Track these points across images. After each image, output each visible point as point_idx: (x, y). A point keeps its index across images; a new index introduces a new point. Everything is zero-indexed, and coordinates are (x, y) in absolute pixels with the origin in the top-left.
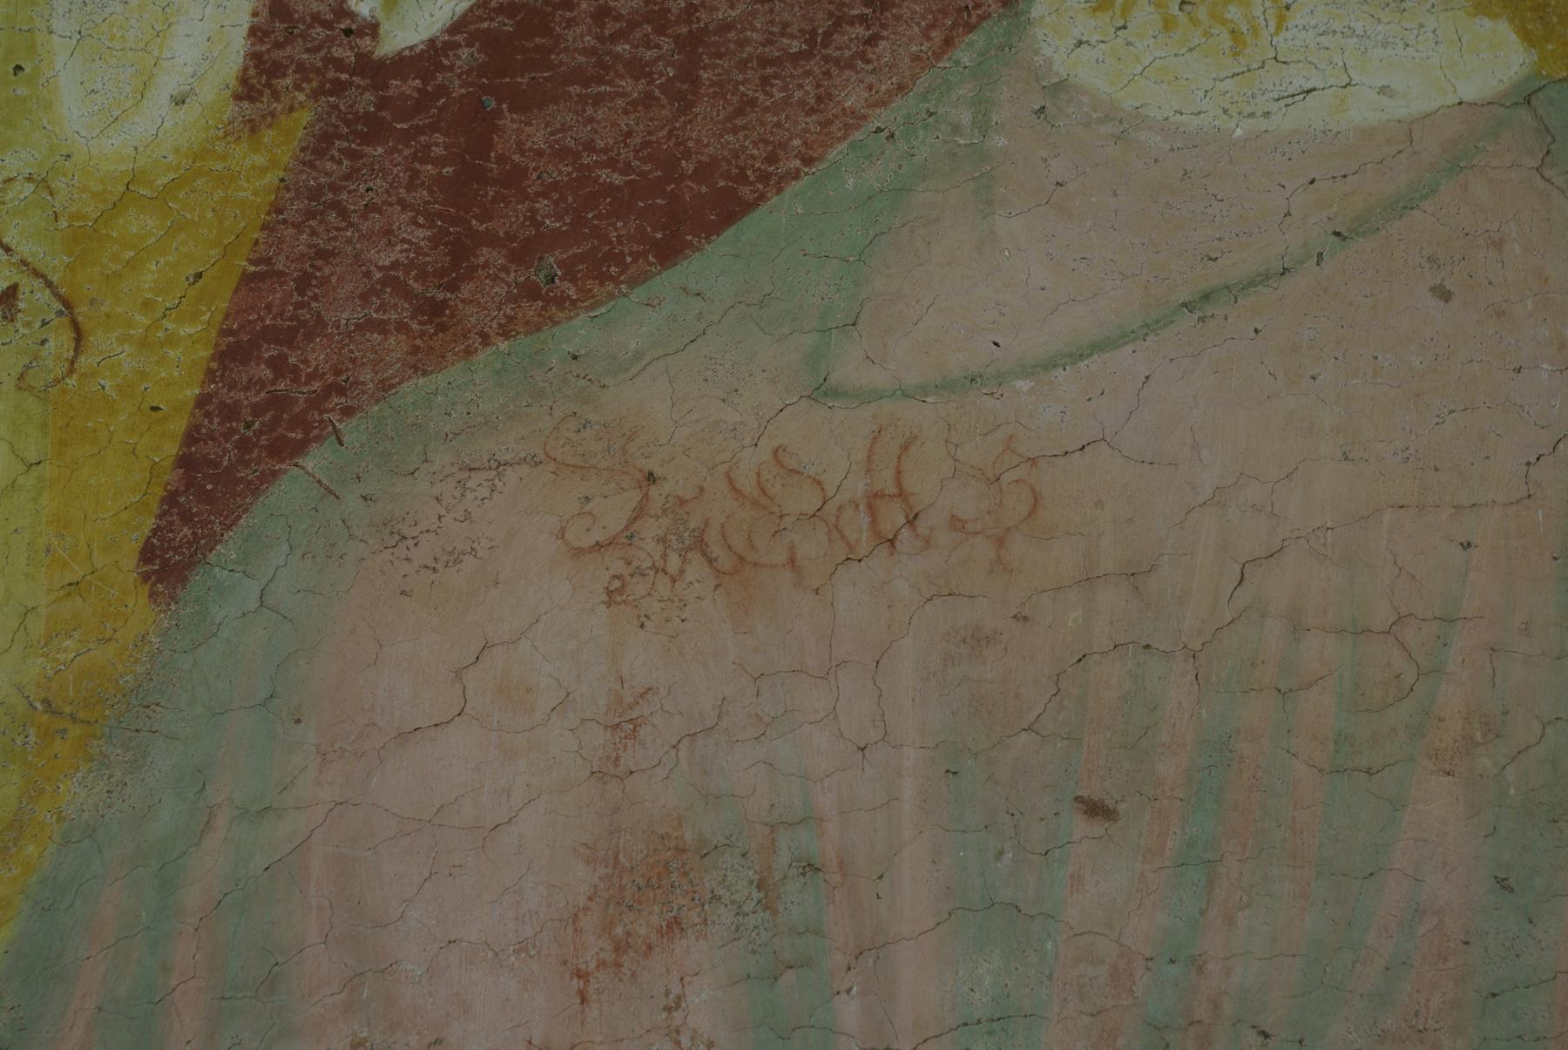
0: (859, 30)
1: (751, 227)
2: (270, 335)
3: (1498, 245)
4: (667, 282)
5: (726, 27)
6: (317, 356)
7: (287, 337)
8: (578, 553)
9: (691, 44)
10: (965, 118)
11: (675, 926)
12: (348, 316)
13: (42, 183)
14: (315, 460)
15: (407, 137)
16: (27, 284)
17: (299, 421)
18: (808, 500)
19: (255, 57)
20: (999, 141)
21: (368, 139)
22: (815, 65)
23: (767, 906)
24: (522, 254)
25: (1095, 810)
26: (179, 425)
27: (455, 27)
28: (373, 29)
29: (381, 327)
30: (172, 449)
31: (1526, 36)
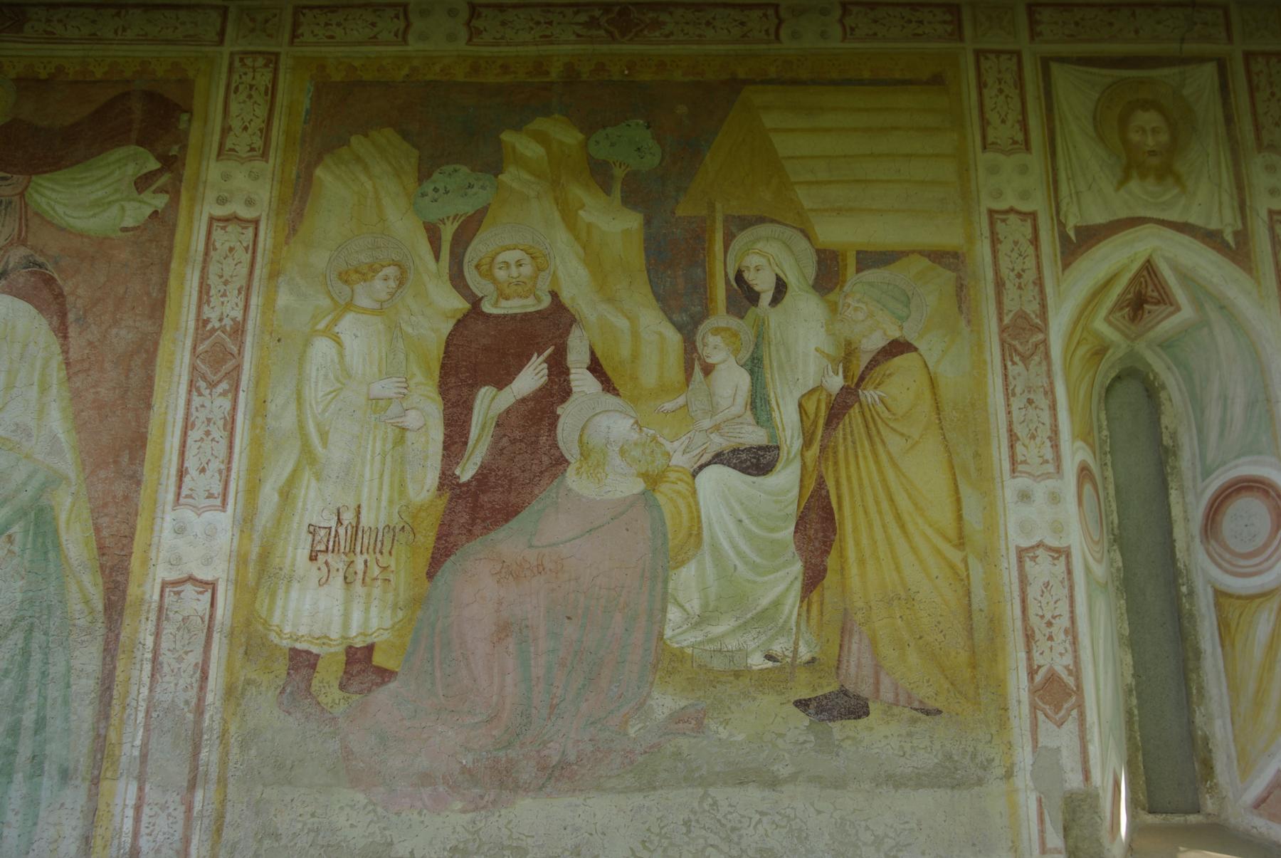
0: (538, 478)
1: (520, 516)
2: (444, 535)
3: (637, 521)
4: (507, 526)
5: (517, 477)
6: (452, 539)
7: (447, 536)
8: (493, 574)
9: (511, 481)
10: (554, 496)
11: (507, 636)
12: (457, 532)
13: (407, 507)
14: (452, 558)
15: (465, 498)
16: (406, 526)
17: (450, 551)
18: (528, 566)
19: (440, 482)
20: (560, 500)
21: (459, 498)
22: (531, 485)
23: (521, 633)
24: (484, 520)
25: (569, 618)
26: (431, 551)
27: (472, 478)
28: (459, 477)
29: (461, 534)
30: (430, 555)
31: (645, 482)
